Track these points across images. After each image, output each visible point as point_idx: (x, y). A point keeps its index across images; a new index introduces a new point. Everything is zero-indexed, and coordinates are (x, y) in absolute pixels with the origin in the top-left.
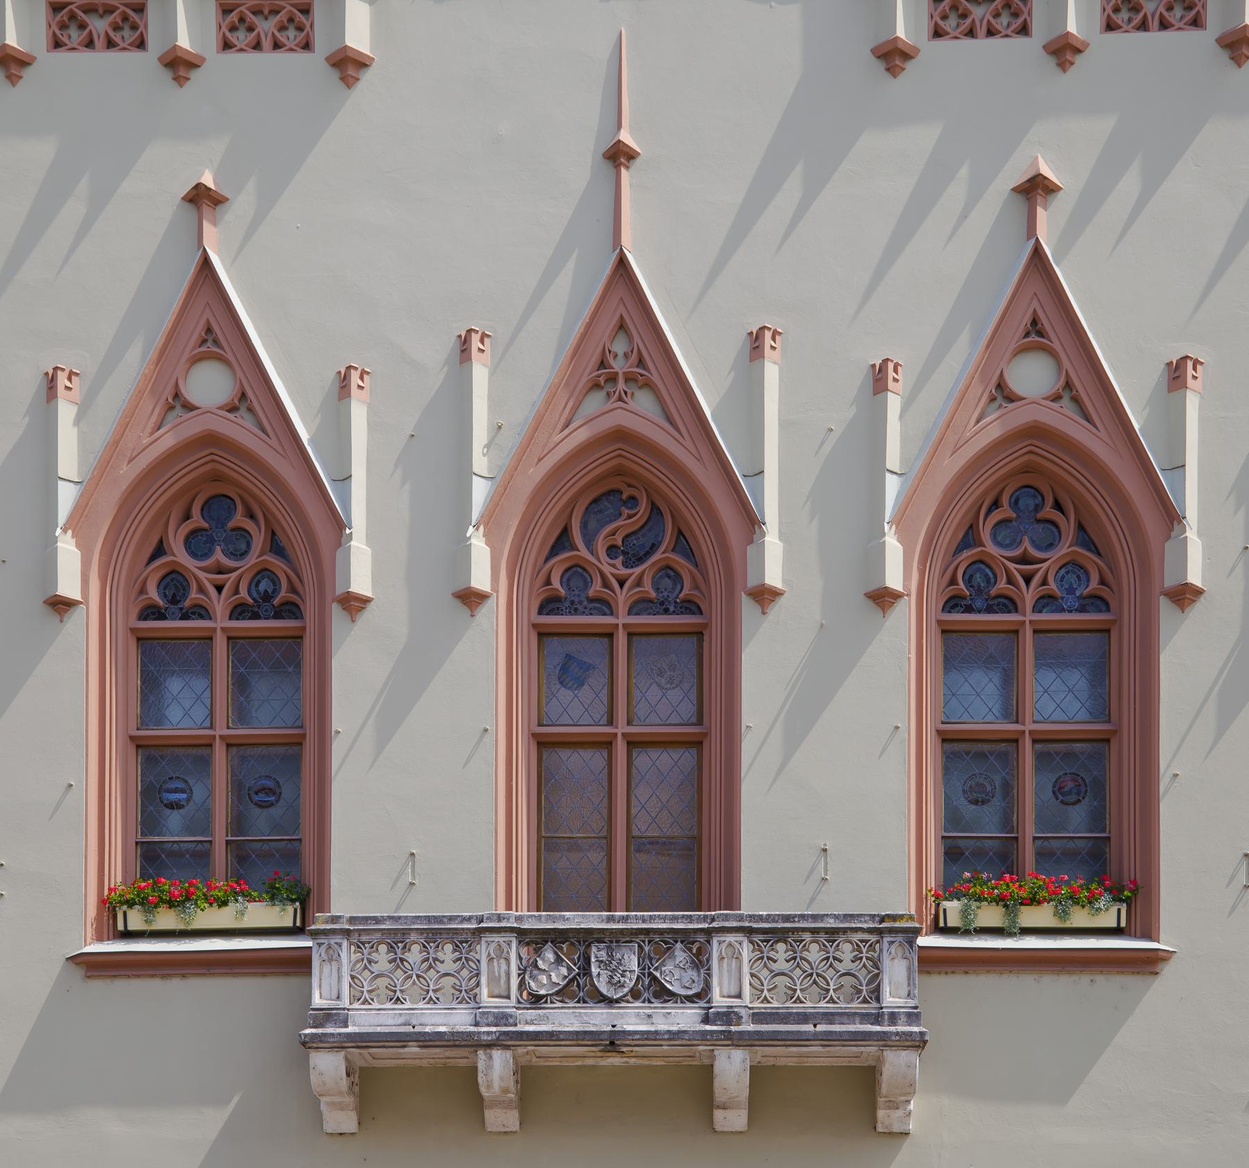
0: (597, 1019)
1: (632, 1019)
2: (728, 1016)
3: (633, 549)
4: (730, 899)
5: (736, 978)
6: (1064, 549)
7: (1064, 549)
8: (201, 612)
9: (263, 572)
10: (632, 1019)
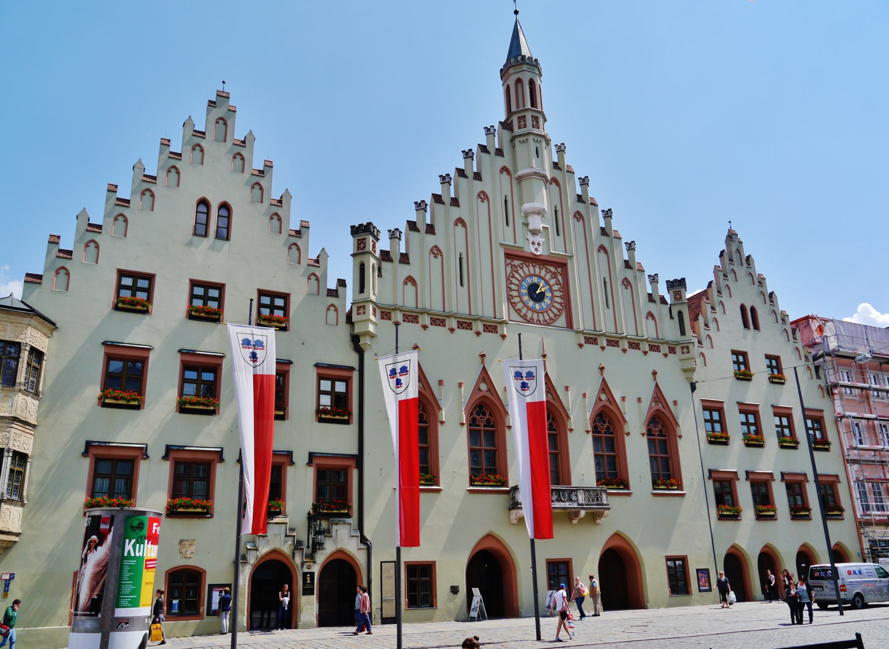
0: (562, 505)
1: (567, 505)
2: (582, 505)
3: (548, 420)
4: (570, 483)
5: (581, 497)
6: (607, 424)
7: (607, 424)
8: (478, 425)
9: (488, 419)
10: (567, 505)
